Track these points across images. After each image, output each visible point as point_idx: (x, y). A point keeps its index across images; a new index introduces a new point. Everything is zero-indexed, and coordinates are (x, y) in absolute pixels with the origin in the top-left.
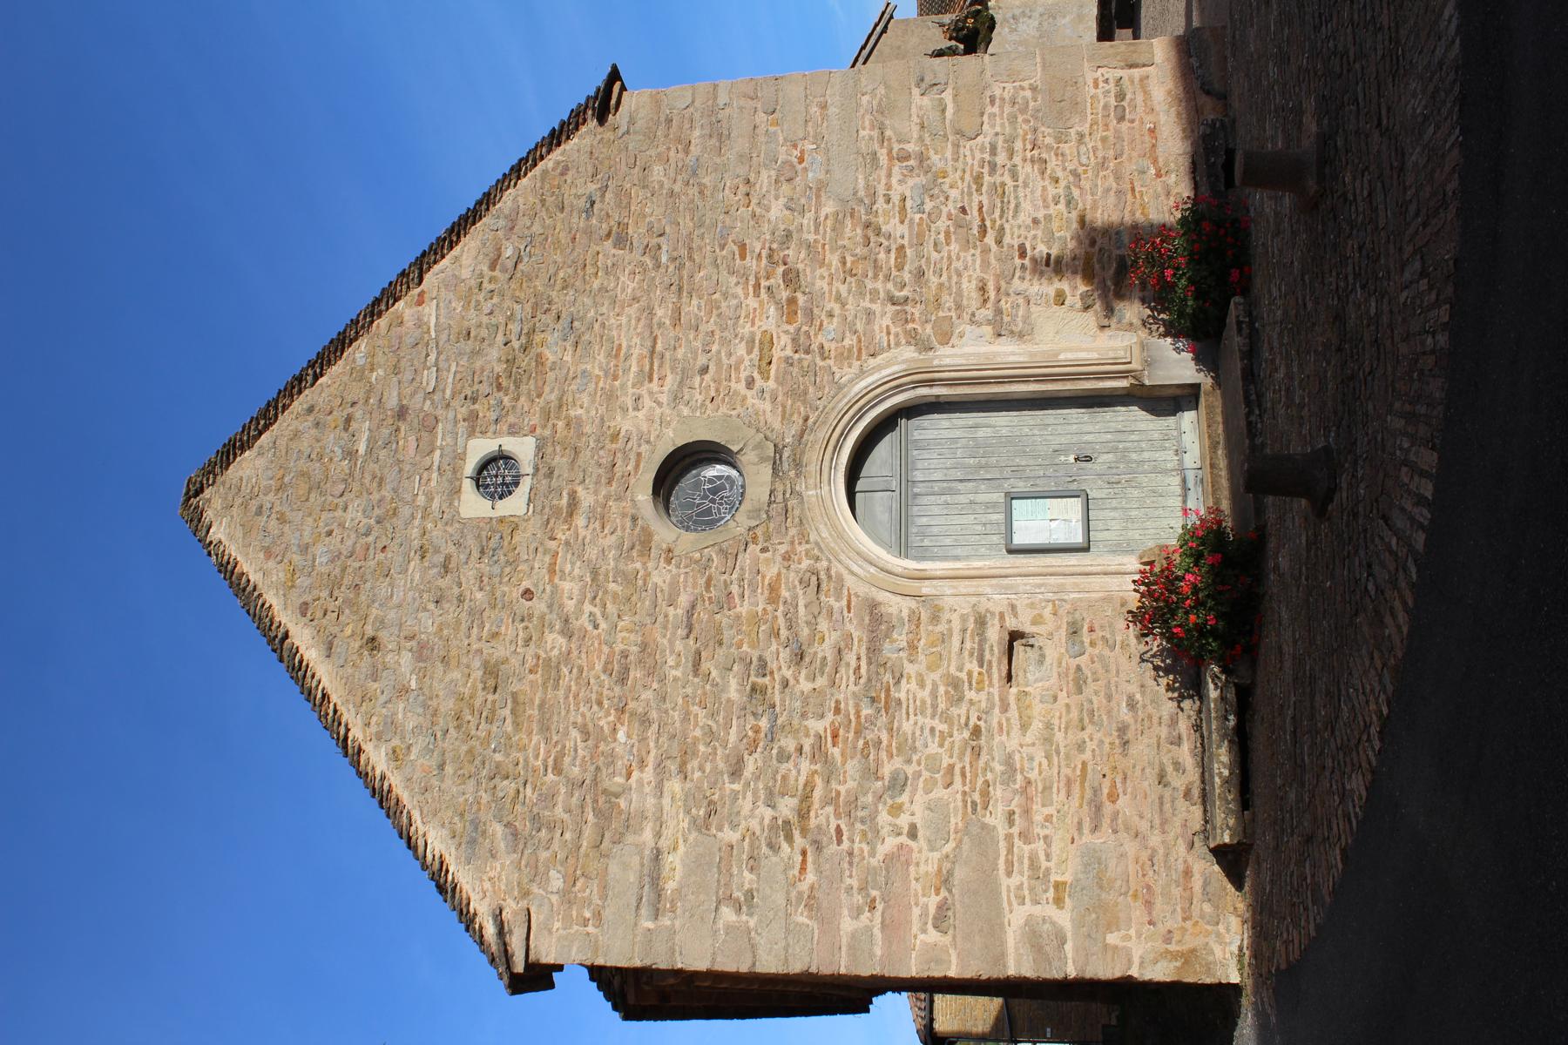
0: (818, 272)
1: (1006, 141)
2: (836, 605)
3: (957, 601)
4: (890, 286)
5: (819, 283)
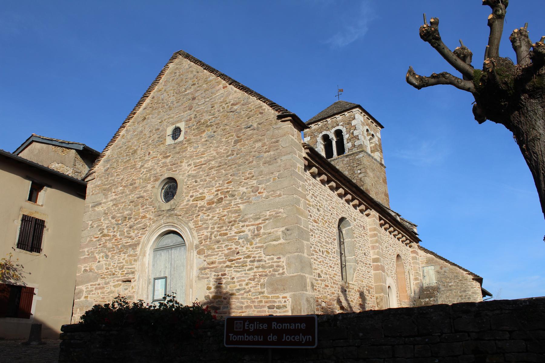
0: (221, 209)
1: (262, 265)
2: (139, 234)
3: (137, 266)
4: (215, 233)
5: (218, 210)
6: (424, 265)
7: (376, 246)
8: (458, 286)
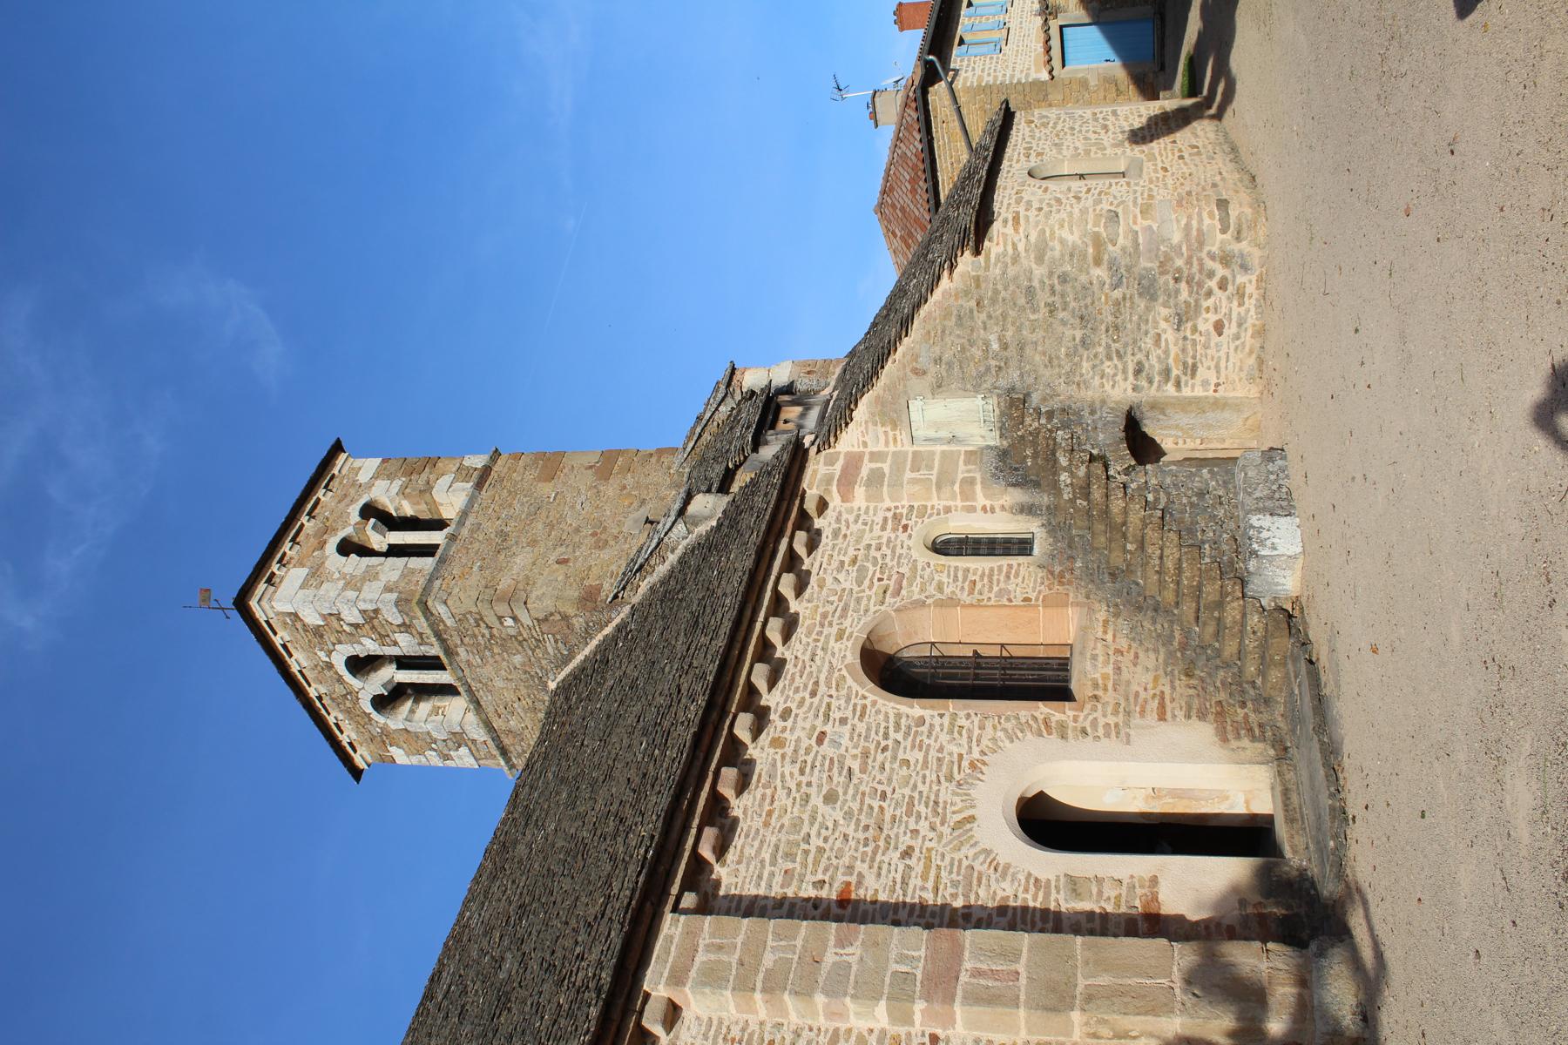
6: (903, 436)
7: (826, 1006)
8: (1004, 316)
